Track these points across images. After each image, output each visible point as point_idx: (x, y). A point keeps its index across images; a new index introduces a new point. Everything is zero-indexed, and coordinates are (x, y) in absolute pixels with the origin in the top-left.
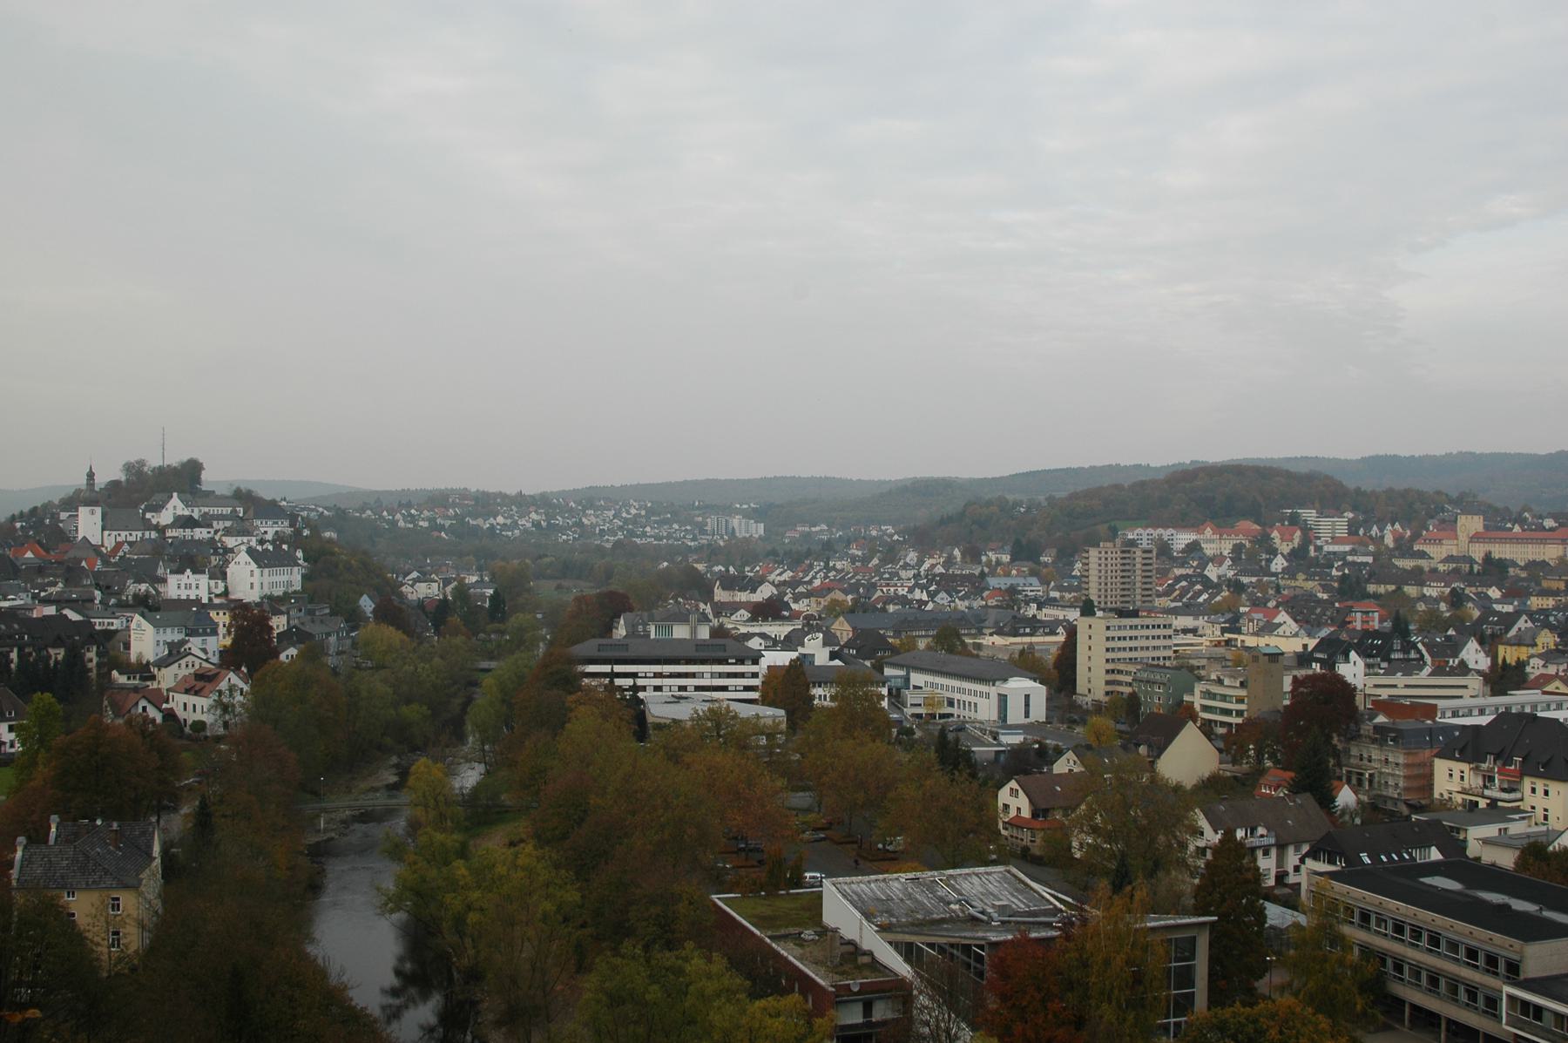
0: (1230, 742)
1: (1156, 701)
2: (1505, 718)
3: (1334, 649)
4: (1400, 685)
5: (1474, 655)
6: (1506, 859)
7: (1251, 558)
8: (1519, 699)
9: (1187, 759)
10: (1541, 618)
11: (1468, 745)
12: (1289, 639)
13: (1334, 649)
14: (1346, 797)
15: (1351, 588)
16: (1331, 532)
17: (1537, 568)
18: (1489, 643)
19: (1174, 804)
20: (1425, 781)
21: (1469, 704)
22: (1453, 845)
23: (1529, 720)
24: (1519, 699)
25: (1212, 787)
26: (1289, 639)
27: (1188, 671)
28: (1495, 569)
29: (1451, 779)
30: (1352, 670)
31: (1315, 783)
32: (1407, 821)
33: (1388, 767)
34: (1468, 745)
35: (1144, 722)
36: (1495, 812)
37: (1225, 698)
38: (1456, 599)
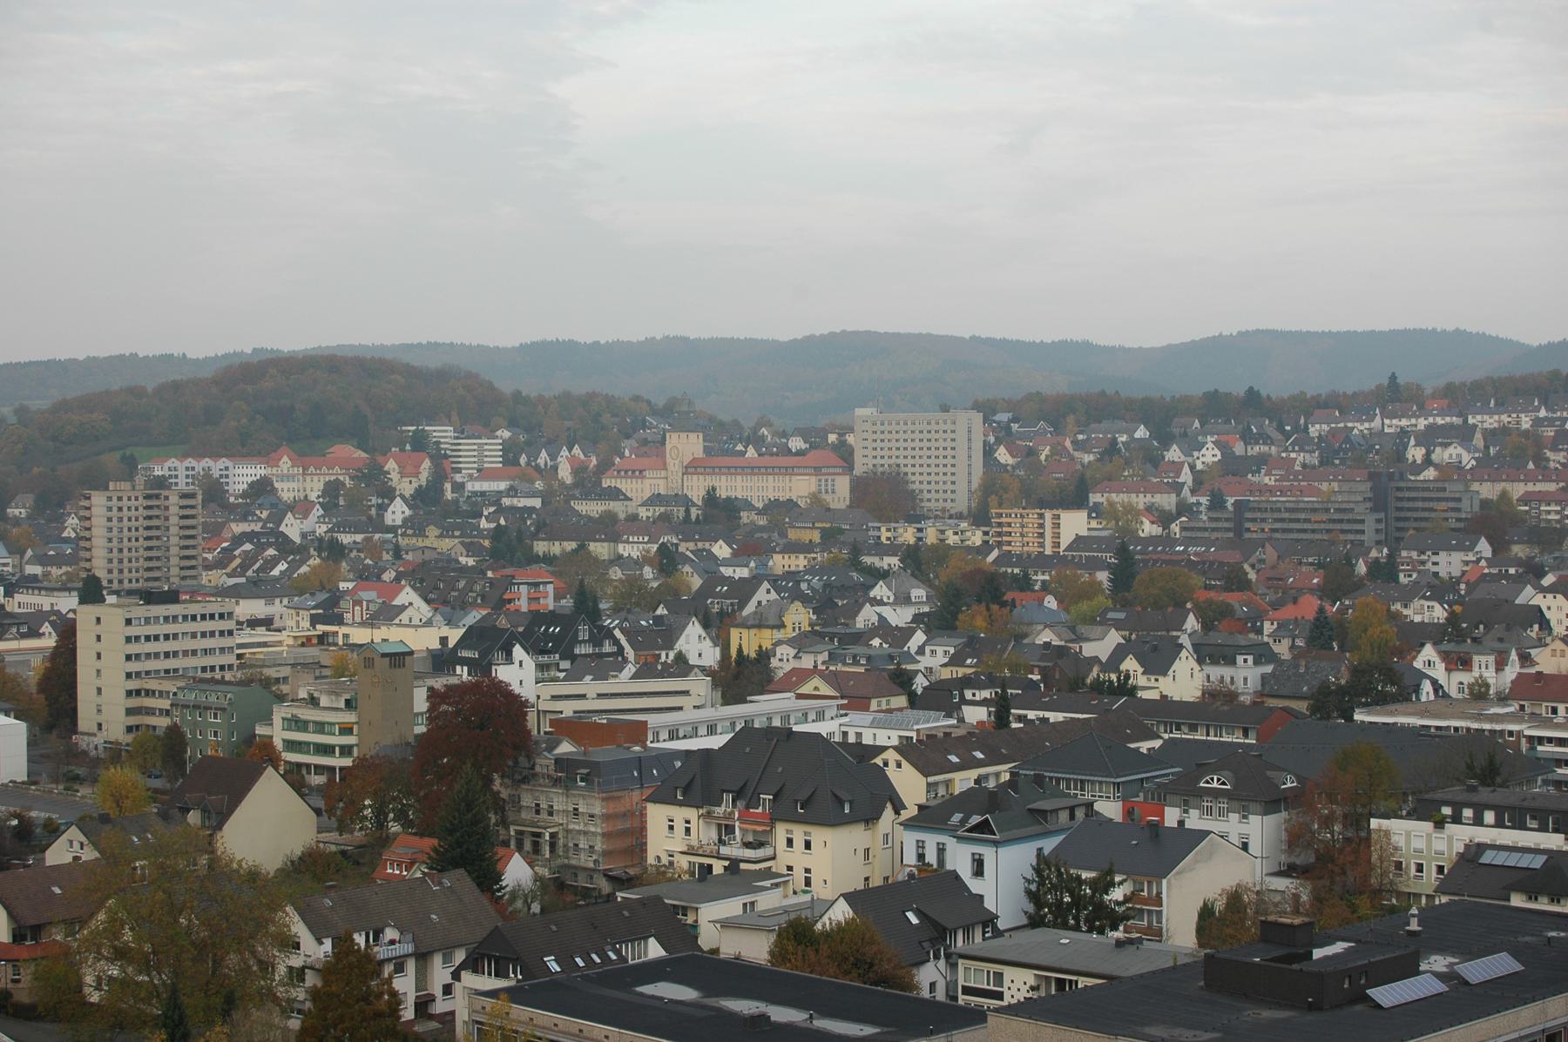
0: (334, 797)
1: (210, 738)
2: (746, 736)
3: (489, 642)
4: (591, 695)
5: (695, 644)
6: (756, 949)
7: (353, 503)
8: (765, 708)
9: (267, 828)
10: (788, 585)
11: (695, 781)
12: (419, 630)
13: (489, 642)
14: (517, 872)
15: (509, 548)
16: (477, 461)
17: (780, 509)
18: (717, 625)
19: (247, 903)
20: (634, 838)
21: (694, 721)
22: (680, 934)
23: (782, 737)
24: (765, 708)
25: (309, 869)
26: (419, 630)
27: (262, 688)
28: (721, 514)
29: (672, 834)
30: (518, 673)
31: (469, 852)
32: (614, 902)
33: (578, 819)
34: (695, 781)
35: (194, 772)
36: (737, 878)
37: (321, 726)
38: (667, 561)
